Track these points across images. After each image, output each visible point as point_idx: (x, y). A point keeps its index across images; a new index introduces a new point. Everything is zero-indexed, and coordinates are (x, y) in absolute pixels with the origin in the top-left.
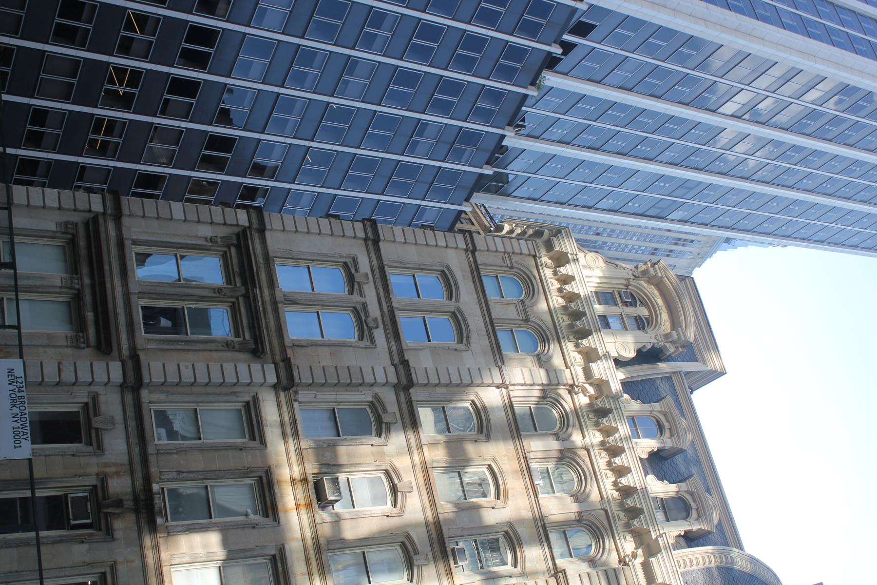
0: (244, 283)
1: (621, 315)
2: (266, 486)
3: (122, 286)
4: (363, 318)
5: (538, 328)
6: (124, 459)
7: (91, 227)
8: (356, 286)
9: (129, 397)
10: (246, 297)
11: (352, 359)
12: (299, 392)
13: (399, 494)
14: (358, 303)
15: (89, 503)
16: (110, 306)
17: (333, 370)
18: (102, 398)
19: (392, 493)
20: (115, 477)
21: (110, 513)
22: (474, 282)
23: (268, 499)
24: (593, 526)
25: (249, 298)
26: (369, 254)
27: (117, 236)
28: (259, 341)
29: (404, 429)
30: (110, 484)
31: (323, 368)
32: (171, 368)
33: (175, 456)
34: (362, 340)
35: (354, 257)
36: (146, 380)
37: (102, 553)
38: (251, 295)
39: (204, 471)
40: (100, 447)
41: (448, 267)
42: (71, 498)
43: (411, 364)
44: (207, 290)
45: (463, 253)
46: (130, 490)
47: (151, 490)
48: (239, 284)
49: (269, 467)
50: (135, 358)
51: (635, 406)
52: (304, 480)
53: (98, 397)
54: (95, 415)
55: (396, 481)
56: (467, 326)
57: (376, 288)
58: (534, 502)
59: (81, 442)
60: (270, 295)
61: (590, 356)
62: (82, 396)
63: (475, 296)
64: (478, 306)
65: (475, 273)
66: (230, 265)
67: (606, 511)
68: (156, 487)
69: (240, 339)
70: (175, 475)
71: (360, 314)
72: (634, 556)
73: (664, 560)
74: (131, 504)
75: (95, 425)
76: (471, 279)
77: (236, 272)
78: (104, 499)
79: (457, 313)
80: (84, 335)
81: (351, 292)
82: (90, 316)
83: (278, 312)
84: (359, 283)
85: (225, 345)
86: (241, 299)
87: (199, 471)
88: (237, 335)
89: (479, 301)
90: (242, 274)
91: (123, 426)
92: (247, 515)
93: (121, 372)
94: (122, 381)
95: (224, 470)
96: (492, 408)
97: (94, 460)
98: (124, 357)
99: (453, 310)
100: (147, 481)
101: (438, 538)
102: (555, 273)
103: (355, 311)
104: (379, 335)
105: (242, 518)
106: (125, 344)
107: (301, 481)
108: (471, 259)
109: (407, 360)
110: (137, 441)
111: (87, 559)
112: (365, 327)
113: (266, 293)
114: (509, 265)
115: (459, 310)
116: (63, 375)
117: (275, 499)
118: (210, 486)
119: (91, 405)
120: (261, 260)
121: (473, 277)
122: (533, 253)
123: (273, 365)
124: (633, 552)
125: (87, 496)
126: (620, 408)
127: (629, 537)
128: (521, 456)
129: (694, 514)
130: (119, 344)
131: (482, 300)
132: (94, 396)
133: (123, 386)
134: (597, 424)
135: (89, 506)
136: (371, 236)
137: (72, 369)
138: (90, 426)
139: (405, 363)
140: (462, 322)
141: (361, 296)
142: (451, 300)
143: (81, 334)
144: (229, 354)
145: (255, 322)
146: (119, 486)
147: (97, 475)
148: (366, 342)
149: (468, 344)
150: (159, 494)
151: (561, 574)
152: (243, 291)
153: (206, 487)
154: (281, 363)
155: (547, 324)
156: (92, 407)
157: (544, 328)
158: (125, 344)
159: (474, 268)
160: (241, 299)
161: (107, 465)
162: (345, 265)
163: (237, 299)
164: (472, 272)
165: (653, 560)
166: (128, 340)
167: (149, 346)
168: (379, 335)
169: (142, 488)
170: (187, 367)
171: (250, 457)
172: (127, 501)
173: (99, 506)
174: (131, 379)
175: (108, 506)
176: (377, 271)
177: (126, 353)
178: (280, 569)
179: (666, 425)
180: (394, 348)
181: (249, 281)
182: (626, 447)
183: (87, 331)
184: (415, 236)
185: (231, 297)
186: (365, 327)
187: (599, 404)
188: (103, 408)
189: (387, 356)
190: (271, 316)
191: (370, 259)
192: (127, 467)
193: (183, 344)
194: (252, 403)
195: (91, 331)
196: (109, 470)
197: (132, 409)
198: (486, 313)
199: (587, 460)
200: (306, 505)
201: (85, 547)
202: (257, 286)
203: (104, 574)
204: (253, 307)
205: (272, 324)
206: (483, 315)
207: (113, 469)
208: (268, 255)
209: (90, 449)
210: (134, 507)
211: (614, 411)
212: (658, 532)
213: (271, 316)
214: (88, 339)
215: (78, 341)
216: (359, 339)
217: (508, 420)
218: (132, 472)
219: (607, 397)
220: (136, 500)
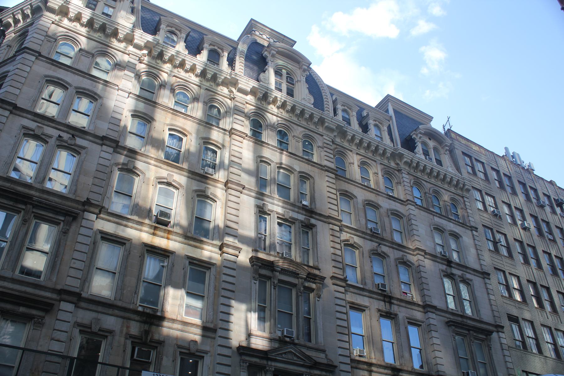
0: (25, 203)
1: (105, 4)
2: (153, 250)
3: (4, 281)
4: (66, 145)
5: (100, 52)
6: (120, 320)
8: (43, 137)
9: (83, 304)
10: (35, 206)
11: (92, 166)
12: (104, 205)
13: (173, 183)
14: (55, 142)
15: (142, 349)
16: (17, 293)
17: (96, 180)
18: (79, 320)
19: (170, 186)
20: (129, 329)
21: (150, 339)
22: (60, 68)
23: (160, 252)
24: (210, 100)
25: (37, 205)
26: (23, 117)
28: (69, 213)
29: (136, 159)
30: (133, 333)
31: (93, 184)
32: (72, 272)
33: (125, 292)
34: (80, 153)
35: (23, 127)
36: (77, 290)
37: (169, 350)
38: (36, 203)
39: (138, 279)
40: (111, 332)
41: (46, 76)
42: (137, 357)
43: (104, 135)
44: (22, 228)
45: (37, 61)
46: (138, 324)
47: (139, 311)
48: (24, 207)
49: (144, 243)
50: (61, 292)
51: (160, 37)
52: (155, 228)
53: (78, 323)
54: (91, 328)
55: (165, 181)
56: (88, 90)
57: (48, 126)
58: (194, 120)
59: (102, 341)
60: (36, 191)
61: (129, 40)
62: (76, 331)
63: (69, 73)
64: (76, 76)
65: (55, 63)
66: (6, 206)
67: (206, 89)
68: (140, 309)
69: (62, 223)
70: (136, 296)
71: (62, 145)
72: (231, 92)
73: (242, 81)
74: (147, 326)
75: (96, 330)
76: (57, 68)
77: (13, 204)
78: (142, 339)
79: (77, 90)
80: (37, 318)
81: (46, 142)
82: (22, 309)
83: (50, 192)
84: (42, 134)
85: (65, 234)
86: (34, 210)
87: (137, 282)
88: (58, 224)
89: (74, 73)
90: (17, 201)
91: (100, 314)
92: (163, 266)
93: (68, 303)
94: (74, 305)
95: (140, 268)
96: (136, 106)
97: (117, 338)
98: (58, 298)
99: (75, 91)
100: (136, 312)
101: (200, 177)
103: (60, 147)
104: (80, 141)
105: (165, 270)
106: (48, 294)
107: (155, 230)
108: (45, 59)
109: (103, 136)
110: (111, 310)
111: (171, 359)
112: (73, 147)
113: (34, 193)
114: (54, 41)
115: (76, 88)
116: (62, 340)
117: (161, 248)
118: (144, 279)
119: (82, 328)
120: (8, 185)
121: (56, 66)
122: (51, 22)
123: (85, 213)
124: (229, 91)
125: (138, 348)
126: (163, 45)
127: (221, 87)
128: (169, 110)
129: (220, 51)
130: (48, 298)
131: (74, 71)
132: (77, 325)
133: (77, 306)
134: (165, 62)
135: (144, 349)
136: (11, 108)
137: (59, 333)
138: (95, 334)
139: (104, 138)
140: (84, 91)
141: (51, 137)
142: (68, 88)
143: (36, 319)
144: (70, 234)
145: (56, 209)
146: (135, 328)
147: (126, 339)
148: (83, 152)
149: (100, 97)
150: (144, 309)
151: (233, 131)
152: (29, 207)
153: (143, 281)
154: (86, 207)
155: (99, 47)
156: (84, 329)
157: (100, 49)
158: (48, 294)
159: (51, 62)
160: (34, 210)
161: (121, 332)
162: (25, 135)
163: (33, 212)
165: (240, 86)
166: (46, 291)
167: (54, 279)
168: (80, 141)
169: (139, 317)
170: (74, 263)
171: (134, 251)
172: (144, 327)
173: (144, 344)
174: (75, 299)
175: (147, 338)
176: (36, 119)
177: (54, 296)
178: (197, 262)
179: (173, 29)
180: (91, 138)
181: (26, 200)
182: (184, 58)
183: (33, 315)
184: (17, 81)
185: (31, 215)
186: (73, 147)
187: (155, 53)
188: (86, 321)
189: (95, 145)
190: (51, 198)
191: (26, 118)
192: (125, 320)
193: (57, 259)
194: (103, 235)
195: (34, 312)
196: (124, 332)
197: (91, 305)
198: (83, 75)
199: (178, 80)
200: (168, 234)
201: (164, 358)
202: (32, 197)
203: (180, 352)
204: (45, 206)
205: (56, 200)
206: (83, 77)
207: (125, 329)
208: (5, 178)
209: (109, 338)
210: (149, 325)
211: (163, 49)
212: (228, 74)
213: (51, 198)
214: (40, 316)
215: (40, 323)
216: (78, 155)
217: (145, 103)
218: (130, 319)
219: (154, 47)
220: (145, 322)
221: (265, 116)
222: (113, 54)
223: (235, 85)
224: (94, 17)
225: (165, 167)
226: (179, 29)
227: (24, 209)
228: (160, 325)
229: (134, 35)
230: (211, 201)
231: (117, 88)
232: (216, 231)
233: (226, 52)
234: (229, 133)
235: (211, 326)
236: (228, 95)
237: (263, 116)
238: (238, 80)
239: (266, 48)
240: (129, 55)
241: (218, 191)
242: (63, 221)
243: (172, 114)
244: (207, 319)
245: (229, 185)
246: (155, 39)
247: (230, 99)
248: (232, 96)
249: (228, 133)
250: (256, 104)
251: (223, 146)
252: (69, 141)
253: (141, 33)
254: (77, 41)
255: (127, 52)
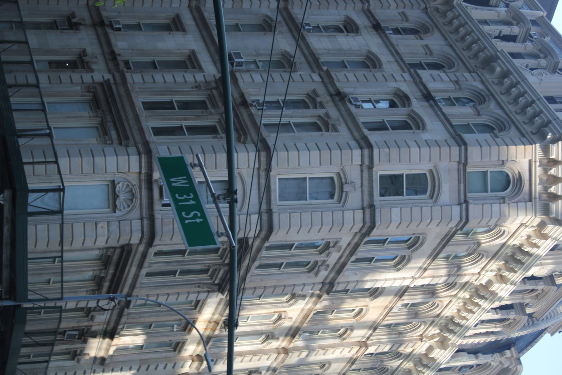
7: (124, 255)
13: (280, 322)
22: (442, 240)
27: (144, 251)
41: (424, 239)
89: (435, 249)
102: (529, 237)
124: (434, 334)
131: (438, 249)
142: (409, 248)
164: (446, 236)
175: (87, 336)
186: (317, 268)
207: (97, 324)
221: (397, 359)
222: (479, 263)
223: (442, 342)
224: (532, 258)
225: (302, 315)
226: (540, 297)
227: (224, 261)
228: (104, 338)
229: (506, 284)
230: (263, 339)
231: (417, 276)
232: (221, 349)
233: (503, 330)
234: (364, 341)
235: (107, 362)
236: (427, 334)
237: (397, 357)
238: (446, 350)
239: (515, 356)
240: (479, 273)
241: (275, 344)
242: (214, 282)
243: (386, 307)
244: (115, 358)
245: (282, 356)
246: (538, 257)
247: (421, 335)
248: (424, 339)
249: (364, 340)
250: (414, 355)
251: (344, 339)
252: (324, 267)
253: (509, 290)
254: (477, 262)
255: (483, 272)
